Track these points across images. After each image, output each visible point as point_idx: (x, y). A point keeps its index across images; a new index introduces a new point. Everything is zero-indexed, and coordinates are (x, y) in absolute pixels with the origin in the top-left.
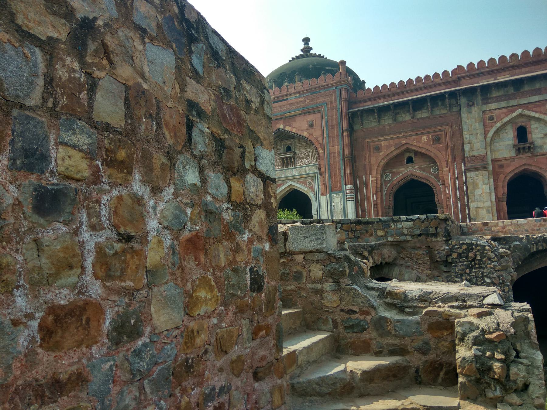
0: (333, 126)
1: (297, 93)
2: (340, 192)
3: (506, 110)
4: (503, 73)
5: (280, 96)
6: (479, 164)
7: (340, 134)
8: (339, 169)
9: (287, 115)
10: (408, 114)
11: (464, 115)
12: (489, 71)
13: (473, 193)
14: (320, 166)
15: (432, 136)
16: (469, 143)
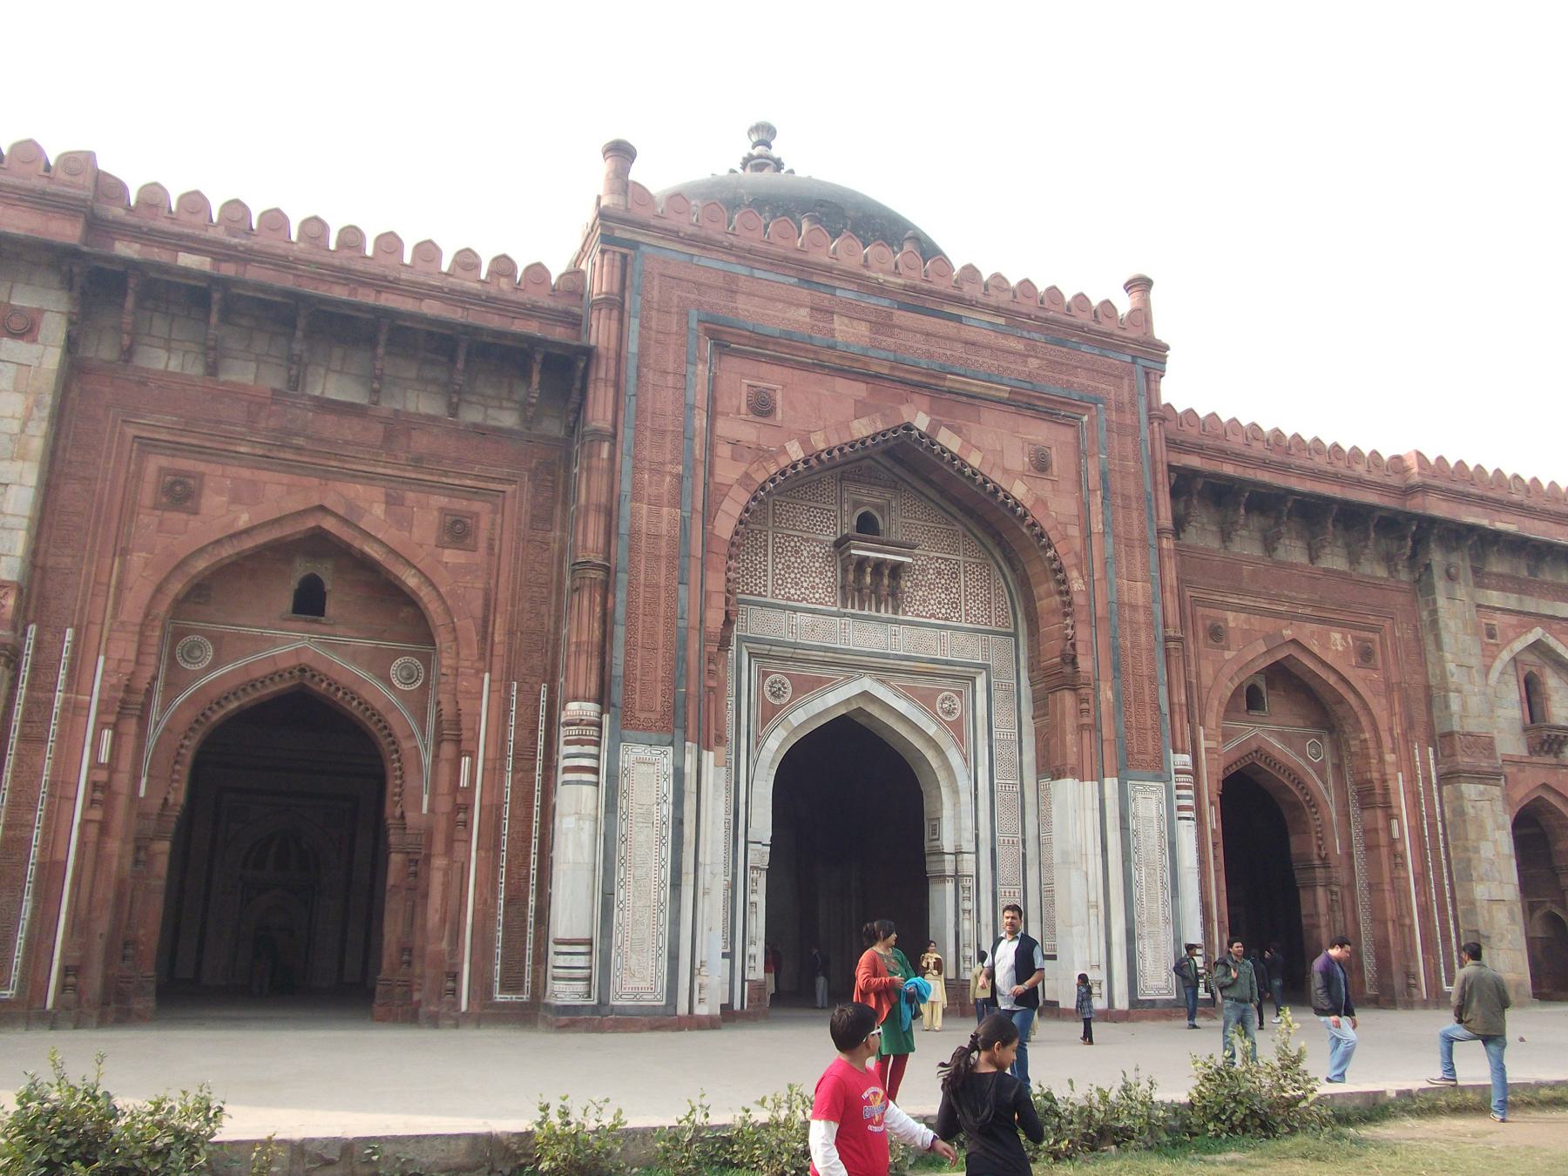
0: (1125, 497)
1: (998, 311)
2: (1158, 778)
3: (1513, 620)
4: (1504, 516)
5: (930, 293)
6: (1484, 764)
7: (1153, 541)
8: (1153, 679)
9: (952, 381)
10: (1300, 544)
11: (1442, 602)
12: (1481, 498)
13: (1477, 850)
14: (1073, 645)
15: (1354, 638)
16: (1459, 691)
